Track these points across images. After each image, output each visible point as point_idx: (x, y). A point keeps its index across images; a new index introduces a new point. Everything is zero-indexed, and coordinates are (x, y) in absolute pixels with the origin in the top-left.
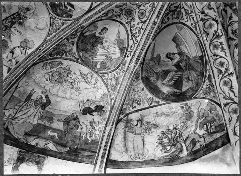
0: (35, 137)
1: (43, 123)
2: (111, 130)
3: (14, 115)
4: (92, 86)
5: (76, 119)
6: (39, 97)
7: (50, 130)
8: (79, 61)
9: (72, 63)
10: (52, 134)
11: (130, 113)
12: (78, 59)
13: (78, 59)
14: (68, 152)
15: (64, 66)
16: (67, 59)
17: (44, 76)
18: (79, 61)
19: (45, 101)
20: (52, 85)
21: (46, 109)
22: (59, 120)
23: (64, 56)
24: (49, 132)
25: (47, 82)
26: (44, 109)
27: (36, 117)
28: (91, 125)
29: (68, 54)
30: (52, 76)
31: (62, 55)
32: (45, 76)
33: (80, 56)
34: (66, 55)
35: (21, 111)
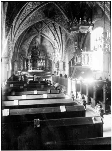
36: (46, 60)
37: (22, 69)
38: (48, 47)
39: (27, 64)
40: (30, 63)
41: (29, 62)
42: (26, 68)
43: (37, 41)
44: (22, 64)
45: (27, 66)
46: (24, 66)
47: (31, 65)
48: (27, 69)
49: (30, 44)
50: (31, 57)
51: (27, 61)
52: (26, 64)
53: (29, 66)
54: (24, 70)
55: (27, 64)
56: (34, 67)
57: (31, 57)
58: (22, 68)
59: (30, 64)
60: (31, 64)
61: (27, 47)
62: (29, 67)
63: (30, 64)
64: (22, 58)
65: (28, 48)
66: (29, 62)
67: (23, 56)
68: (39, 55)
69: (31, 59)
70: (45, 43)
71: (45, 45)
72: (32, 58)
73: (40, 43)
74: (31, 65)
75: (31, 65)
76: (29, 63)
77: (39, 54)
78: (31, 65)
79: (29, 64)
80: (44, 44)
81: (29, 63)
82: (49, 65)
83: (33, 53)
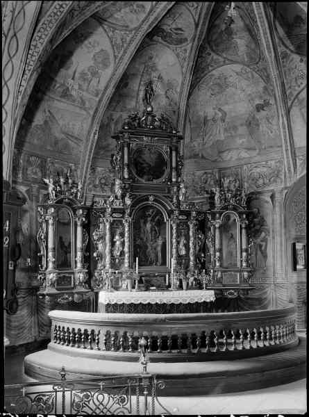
2: (283, 123)
4: (251, 81)
5: (254, 118)
6: (214, 114)
11: (298, 94)
13: (224, 61)
14: (259, 154)
15: (217, 76)
16: (214, 69)
22: (242, 125)
23: (210, 68)
28: (268, 121)
30: (213, 90)
31: (208, 68)
33: (225, 58)
34: (212, 66)
37: (47, 283)
38: (235, 128)
39: (89, 248)
40: (113, 236)
42: (81, 277)
44: (50, 245)
45: (90, 261)
46: (63, 263)
47: (117, 253)
50: (123, 189)
52: (79, 245)
53: (101, 256)
55: (89, 248)
57: (119, 192)
58: (52, 276)
59: (113, 244)
60: (124, 243)
61: (86, 126)
62: (104, 269)
63: (113, 244)
64: (52, 195)
65: (96, 127)
67: (56, 183)
69: (118, 204)
71: (210, 112)
72: (128, 202)
74: (122, 253)
75: (122, 253)
76: (102, 238)
78: (117, 253)
79: (103, 248)
80: (206, 104)
81: (108, 237)
83: (137, 165)
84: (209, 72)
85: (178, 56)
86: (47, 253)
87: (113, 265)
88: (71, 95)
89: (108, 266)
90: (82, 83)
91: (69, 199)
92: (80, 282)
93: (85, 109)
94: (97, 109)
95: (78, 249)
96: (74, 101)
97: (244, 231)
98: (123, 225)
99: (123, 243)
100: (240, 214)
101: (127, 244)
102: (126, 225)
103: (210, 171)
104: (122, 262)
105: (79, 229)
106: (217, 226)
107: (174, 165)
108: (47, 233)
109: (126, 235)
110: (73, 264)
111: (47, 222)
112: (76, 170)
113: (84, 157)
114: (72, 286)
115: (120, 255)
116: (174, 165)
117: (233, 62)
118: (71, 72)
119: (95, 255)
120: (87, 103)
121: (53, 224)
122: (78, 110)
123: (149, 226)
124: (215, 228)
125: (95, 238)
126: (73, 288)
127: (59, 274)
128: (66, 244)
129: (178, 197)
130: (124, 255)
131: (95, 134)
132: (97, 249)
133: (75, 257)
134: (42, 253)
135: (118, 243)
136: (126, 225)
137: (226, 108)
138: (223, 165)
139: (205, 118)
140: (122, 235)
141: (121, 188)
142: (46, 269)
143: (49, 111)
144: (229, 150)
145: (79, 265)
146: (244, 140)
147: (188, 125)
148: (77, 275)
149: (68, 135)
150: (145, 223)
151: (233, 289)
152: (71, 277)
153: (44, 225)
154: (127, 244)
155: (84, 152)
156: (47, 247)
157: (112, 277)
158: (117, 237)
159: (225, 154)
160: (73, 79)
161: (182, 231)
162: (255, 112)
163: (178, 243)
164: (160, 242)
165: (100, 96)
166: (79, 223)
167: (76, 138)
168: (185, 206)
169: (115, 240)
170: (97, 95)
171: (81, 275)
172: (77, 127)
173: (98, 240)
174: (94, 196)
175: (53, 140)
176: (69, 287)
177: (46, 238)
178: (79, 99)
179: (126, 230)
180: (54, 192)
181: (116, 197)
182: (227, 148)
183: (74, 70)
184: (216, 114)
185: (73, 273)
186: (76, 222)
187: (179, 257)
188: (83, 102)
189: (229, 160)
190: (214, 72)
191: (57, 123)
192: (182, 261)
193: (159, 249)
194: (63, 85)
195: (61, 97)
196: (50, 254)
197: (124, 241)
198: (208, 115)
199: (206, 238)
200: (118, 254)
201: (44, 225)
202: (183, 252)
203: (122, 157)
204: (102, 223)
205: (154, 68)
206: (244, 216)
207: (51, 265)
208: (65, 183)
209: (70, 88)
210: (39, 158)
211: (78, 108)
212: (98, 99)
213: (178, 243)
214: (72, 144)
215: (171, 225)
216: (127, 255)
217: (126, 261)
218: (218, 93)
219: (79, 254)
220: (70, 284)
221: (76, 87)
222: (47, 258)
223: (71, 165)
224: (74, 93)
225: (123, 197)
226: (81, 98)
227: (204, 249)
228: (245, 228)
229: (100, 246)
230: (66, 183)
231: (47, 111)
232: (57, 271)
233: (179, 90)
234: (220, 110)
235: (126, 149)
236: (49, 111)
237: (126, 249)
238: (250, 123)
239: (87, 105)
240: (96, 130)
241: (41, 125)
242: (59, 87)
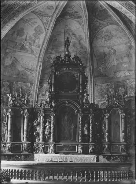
0: (119, 72)
1: (119, 62)
3: (104, 67)
6: (109, 51)
7: (124, 64)
8: (109, 24)
9: (107, 27)
10: (125, 66)
12: (107, 24)
13: (107, 24)
15: (105, 31)
16: (102, 28)
17: (102, 42)
18: (109, 24)
19: (113, 51)
20: (109, 42)
21: (116, 54)
22: (125, 56)
23: (100, 28)
24: (124, 66)
25: (105, 43)
26: (115, 54)
27: (115, 61)
29: (101, 26)
30: (105, 39)
31: (99, 28)
32: (103, 41)
33: (107, 22)
34: (101, 27)
35: (106, 63)
36: (115, 112)
38: (122, 58)
39: (31, 129)
40: (45, 122)
41: (41, 119)
43: (74, 34)
45: (32, 138)
47: (46, 133)
48: (32, 150)
49: (45, 45)
51: (33, 116)
52: (25, 128)
53: (38, 134)
54: (15, 154)
55: (31, 129)
56: (62, 143)
59: (44, 128)
60: (50, 127)
62: (40, 142)
63: (44, 128)
65: (40, 64)
66: (41, 119)
68: (83, 92)
70: (108, 44)
71: (107, 50)
72: (53, 105)
73: (86, 43)
74: (50, 133)
75: (50, 133)
76: (39, 124)
77: (84, 87)
78: (46, 133)
79: (40, 130)
80: (102, 45)
82: (125, 132)
84: (100, 30)
85: (80, 24)
86: (7, 133)
87: (44, 140)
88: (26, 48)
89: (41, 140)
90: (31, 42)
91: (20, 104)
92: (25, 149)
93: (34, 54)
94: (40, 55)
95: (25, 131)
96: (28, 51)
97: (123, 119)
98: (51, 117)
99: (50, 128)
100: (121, 109)
101: (52, 128)
102: (52, 117)
103: (110, 84)
104: (49, 138)
105: (26, 120)
106: (107, 117)
107: (81, 83)
108: (8, 122)
109: (52, 122)
110: (22, 139)
111: (8, 116)
112: (31, 87)
113: (35, 79)
114: (21, 151)
115: (49, 135)
116: (81, 83)
117: (111, 24)
118: (24, 37)
119: (34, 134)
120: (34, 51)
121: (11, 118)
122: (30, 55)
123: (66, 118)
124: (106, 118)
125: (35, 124)
126: (22, 152)
127: (12, 144)
128: (19, 128)
129: (82, 101)
130: (51, 134)
131: (40, 67)
132: (36, 130)
133: (23, 135)
134: (5, 132)
135: (47, 127)
136: (52, 117)
137: (115, 48)
138: (117, 80)
139: (104, 53)
140: (50, 123)
141: (49, 97)
142: (7, 141)
143: (14, 57)
144: (120, 71)
145: (25, 139)
146: (127, 65)
147: (94, 59)
148: (23, 145)
149: (26, 68)
150: (64, 116)
151: (117, 156)
152: (20, 146)
153: (7, 118)
154: (52, 128)
155: (35, 77)
156: (7, 129)
157: (43, 146)
158: (47, 124)
159: (117, 73)
160: (26, 40)
161: (85, 120)
162: (129, 50)
163: (83, 127)
164: (73, 127)
165: (40, 48)
166: (25, 116)
167: (31, 70)
168: (86, 106)
169: (46, 125)
170: (39, 47)
171: (25, 145)
172: (30, 64)
173: (37, 125)
174: (42, 100)
175: (17, 72)
176: (20, 151)
177: (7, 124)
178: (30, 50)
179: (52, 120)
180: (11, 101)
181: (46, 102)
182: (119, 70)
183: (25, 36)
184: (110, 51)
185: (22, 144)
186: (24, 116)
187: (83, 135)
188: (32, 51)
189: (120, 77)
190: (103, 29)
191: (20, 63)
192: (85, 138)
193: (72, 130)
194: (21, 44)
195: (20, 50)
196: (9, 133)
197: (51, 126)
198: (106, 52)
199: (101, 124)
200: (48, 133)
201: (7, 118)
202: (86, 133)
203: (51, 80)
204: (39, 116)
205: (70, 30)
206: (123, 111)
207: (9, 139)
208: (18, 96)
209: (25, 45)
210: (9, 82)
211: (30, 54)
212: (40, 49)
213: (83, 127)
214: (28, 73)
215: (79, 117)
216: (52, 134)
217: (52, 137)
218: (108, 39)
219: (25, 133)
220: (20, 150)
221: (28, 44)
222: (7, 135)
223: (28, 84)
224: (27, 47)
225: (50, 102)
226: (31, 49)
227: (101, 131)
228: (124, 118)
229: (38, 129)
230: (19, 95)
231: (13, 57)
232: (12, 142)
233: (85, 41)
234: (112, 48)
235: (53, 75)
236: (14, 57)
237: (52, 131)
238: (128, 55)
239: (35, 52)
240: (40, 65)
241: (10, 65)
242: (18, 45)
